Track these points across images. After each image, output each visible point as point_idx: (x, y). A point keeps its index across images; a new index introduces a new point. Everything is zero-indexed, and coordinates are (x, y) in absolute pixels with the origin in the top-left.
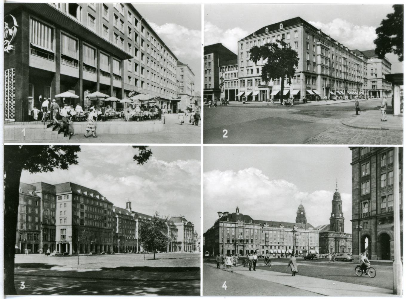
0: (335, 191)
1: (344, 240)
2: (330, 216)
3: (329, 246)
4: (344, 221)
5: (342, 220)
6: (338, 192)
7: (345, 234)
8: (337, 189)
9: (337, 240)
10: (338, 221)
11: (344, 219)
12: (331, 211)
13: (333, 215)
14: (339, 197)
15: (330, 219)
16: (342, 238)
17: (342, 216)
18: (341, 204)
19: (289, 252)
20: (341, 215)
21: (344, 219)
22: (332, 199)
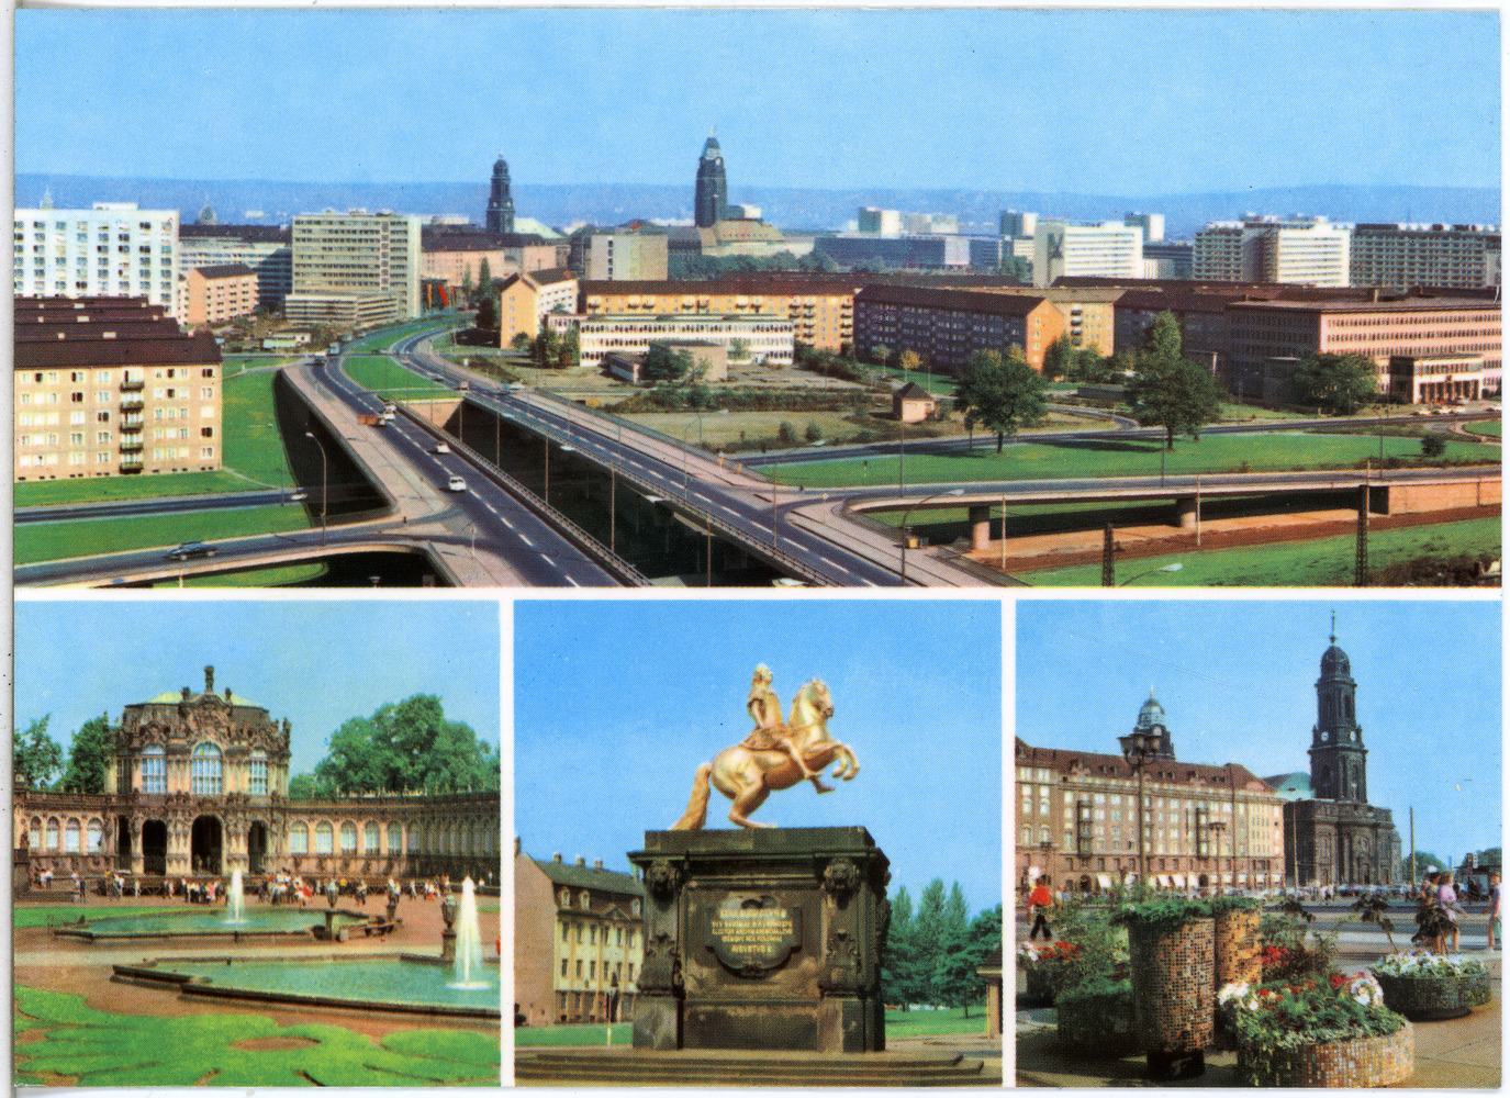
1: (1367, 831)
3: (1318, 858)
5: (1359, 755)
6: (1339, 650)
7: (1371, 809)
8: (1336, 634)
9: (1343, 830)
10: (1344, 759)
11: (1366, 752)
13: (1325, 736)
14: (1346, 667)
15: (1309, 752)
16: (1360, 825)
19: (1158, 883)
20: (1353, 736)
21: (1366, 752)
22: (1318, 675)
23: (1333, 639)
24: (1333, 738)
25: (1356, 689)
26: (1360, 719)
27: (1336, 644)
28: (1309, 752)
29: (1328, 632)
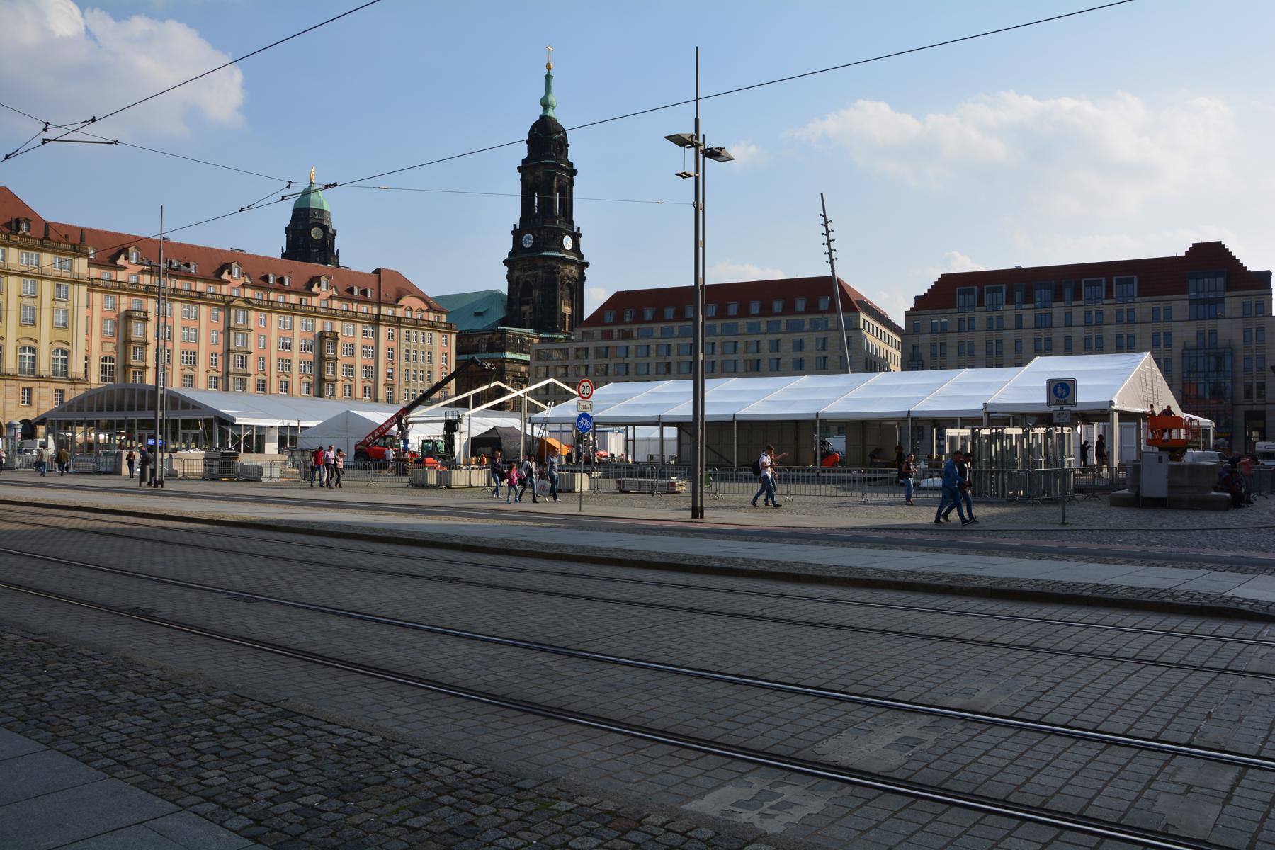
0: (541, 111)
2: (507, 245)
4: (582, 278)
11: (587, 265)
12: (515, 216)
13: (529, 240)
14: (563, 145)
15: (506, 262)
17: (576, 248)
18: (572, 183)
20: (568, 242)
21: (587, 265)
22: (522, 152)
23: (546, 104)
24: (538, 247)
25: (576, 178)
26: (579, 219)
27: (550, 113)
28: (506, 262)
29: (543, 94)
